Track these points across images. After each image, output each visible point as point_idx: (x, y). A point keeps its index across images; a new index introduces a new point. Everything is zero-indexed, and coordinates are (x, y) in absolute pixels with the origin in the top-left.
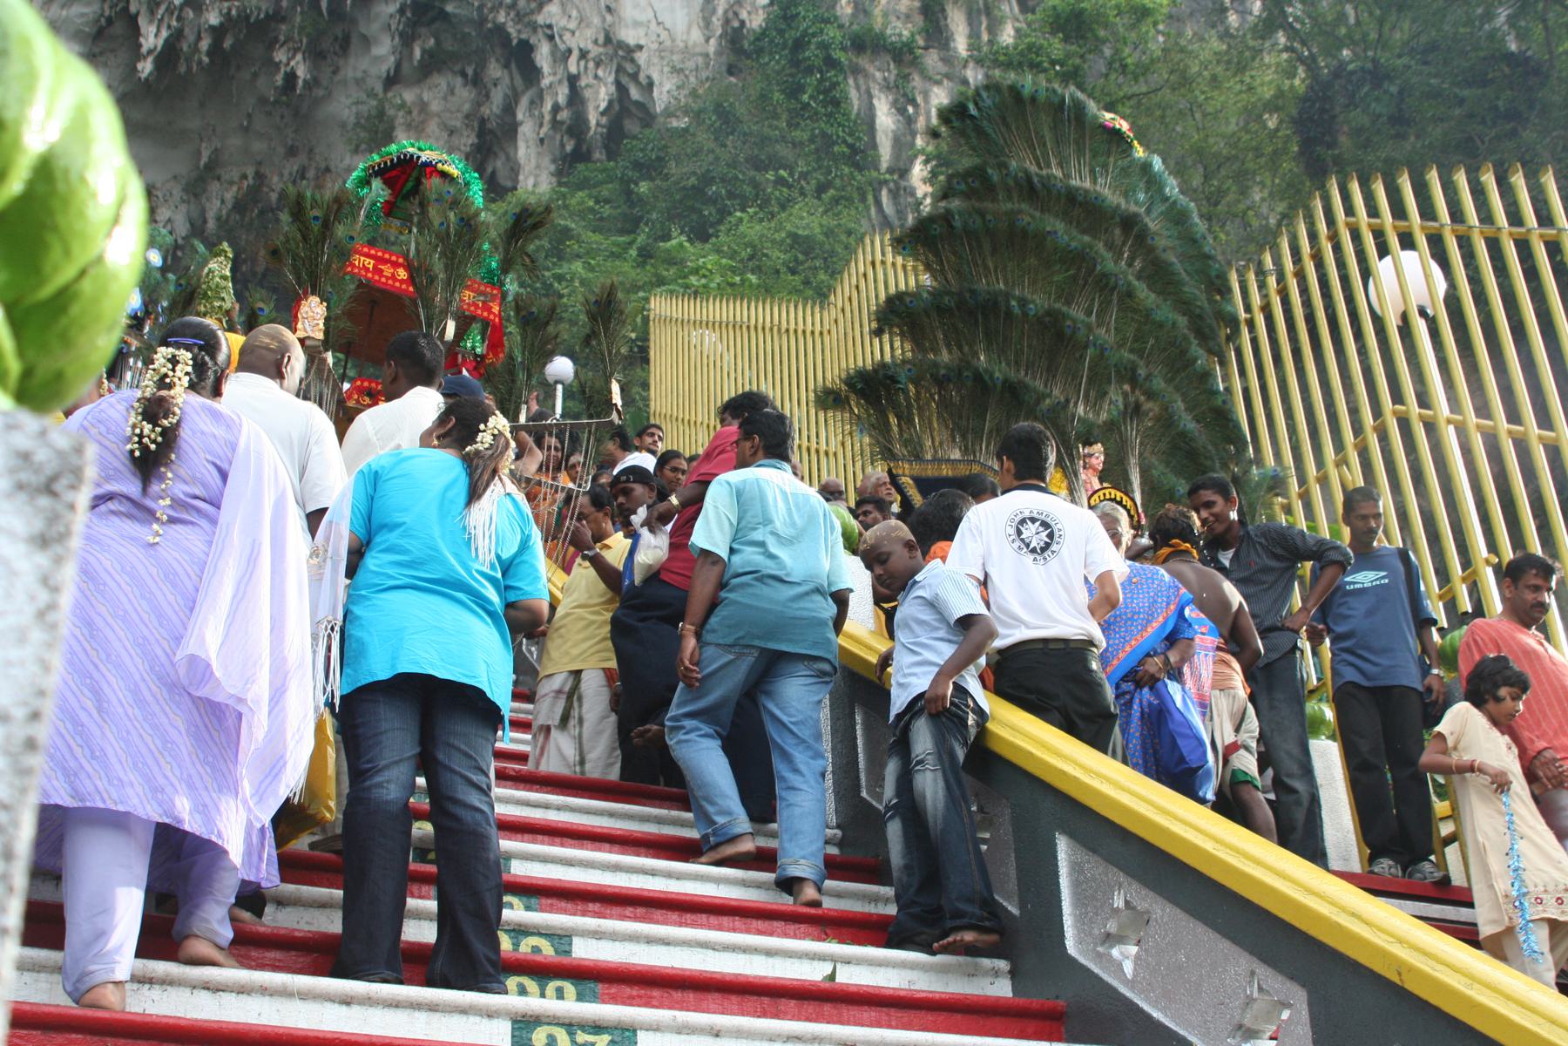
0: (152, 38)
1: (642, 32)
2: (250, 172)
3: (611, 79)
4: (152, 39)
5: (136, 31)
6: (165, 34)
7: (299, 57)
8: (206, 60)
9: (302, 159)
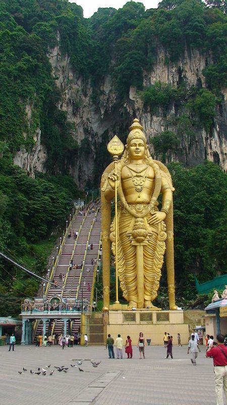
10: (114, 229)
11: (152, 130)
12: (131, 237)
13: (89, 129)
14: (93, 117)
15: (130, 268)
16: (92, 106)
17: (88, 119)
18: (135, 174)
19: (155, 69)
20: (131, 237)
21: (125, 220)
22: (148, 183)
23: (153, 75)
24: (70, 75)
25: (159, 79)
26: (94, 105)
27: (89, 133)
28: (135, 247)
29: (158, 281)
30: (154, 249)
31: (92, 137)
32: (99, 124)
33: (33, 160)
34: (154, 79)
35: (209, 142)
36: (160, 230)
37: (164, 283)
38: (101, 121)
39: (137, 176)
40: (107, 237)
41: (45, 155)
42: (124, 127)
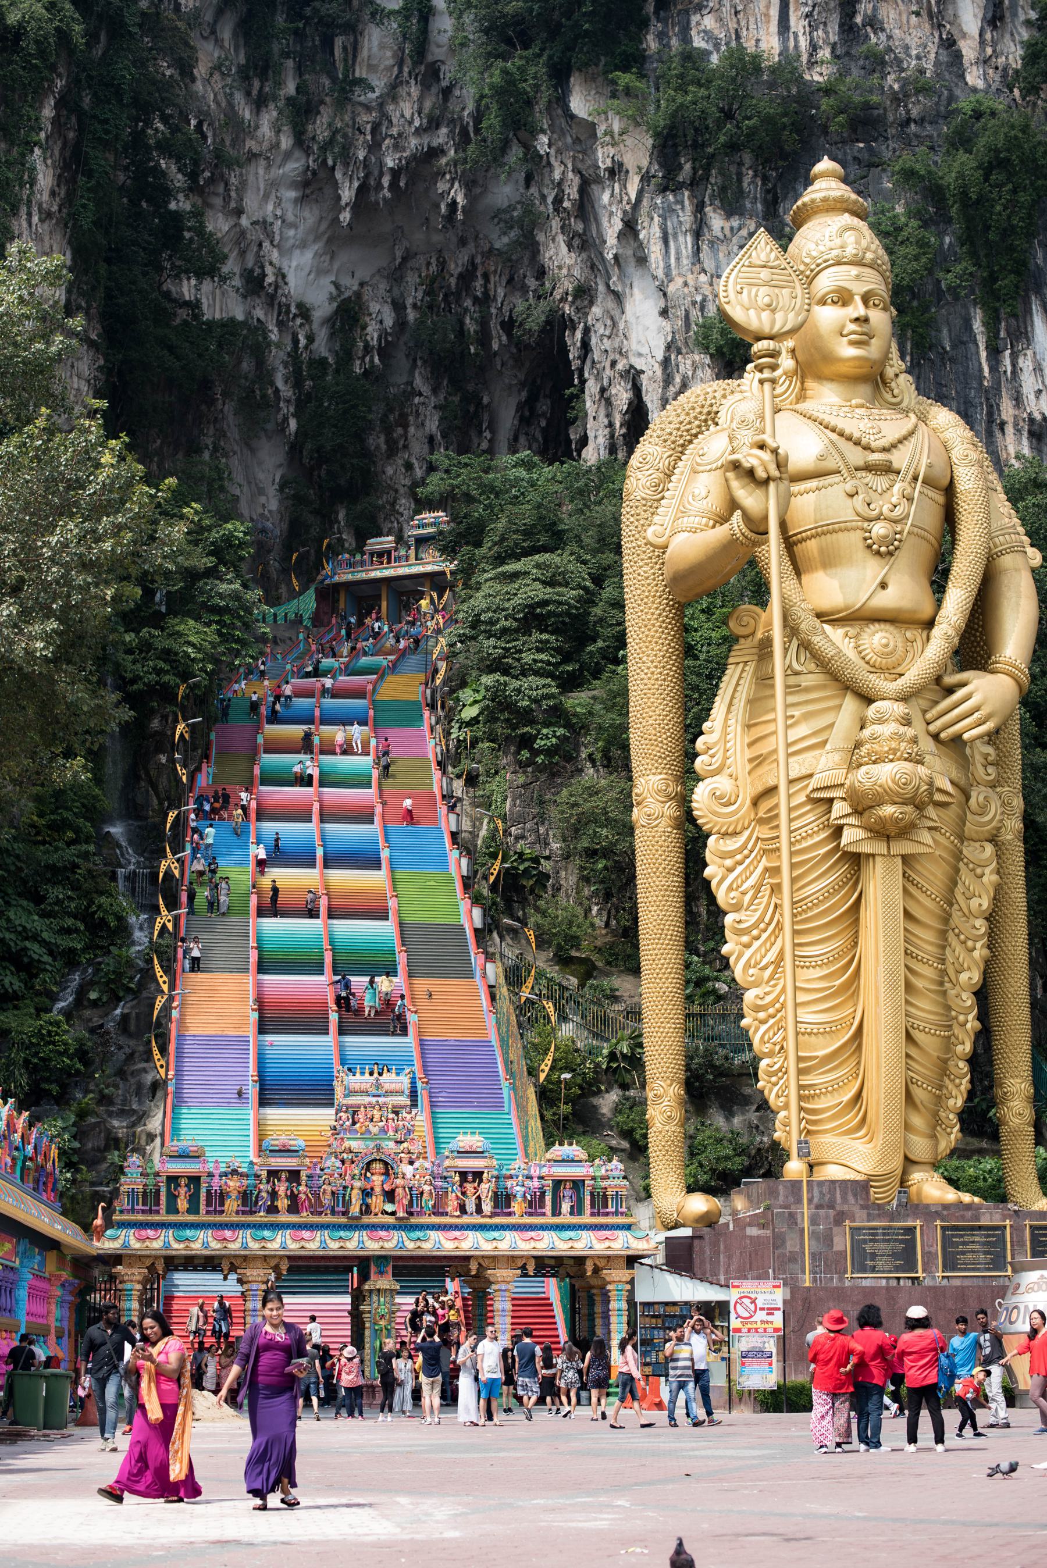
0: (347, 194)
1: (642, 360)
2: (433, 261)
3: (629, 386)
4: (347, 193)
5: (336, 185)
6: (356, 184)
7: (456, 185)
8: (388, 195)
9: (471, 246)
10: (717, 762)
11: (703, 278)
13: (270, 279)
14: (290, 217)
16: (288, 156)
17: (263, 224)
18: (857, 457)
20: (840, 808)
22: (924, 512)
25: (733, 25)
26: (297, 154)
27: (271, 300)
28: (855, 861)
31: (280, 324)
32: (316, 254)
34: (709, 22)
35: (1007, 362)
37: (983, 1064)
38: (334, 240)
39: (868, 468)
40: (670, 810)
42: (453, 281)
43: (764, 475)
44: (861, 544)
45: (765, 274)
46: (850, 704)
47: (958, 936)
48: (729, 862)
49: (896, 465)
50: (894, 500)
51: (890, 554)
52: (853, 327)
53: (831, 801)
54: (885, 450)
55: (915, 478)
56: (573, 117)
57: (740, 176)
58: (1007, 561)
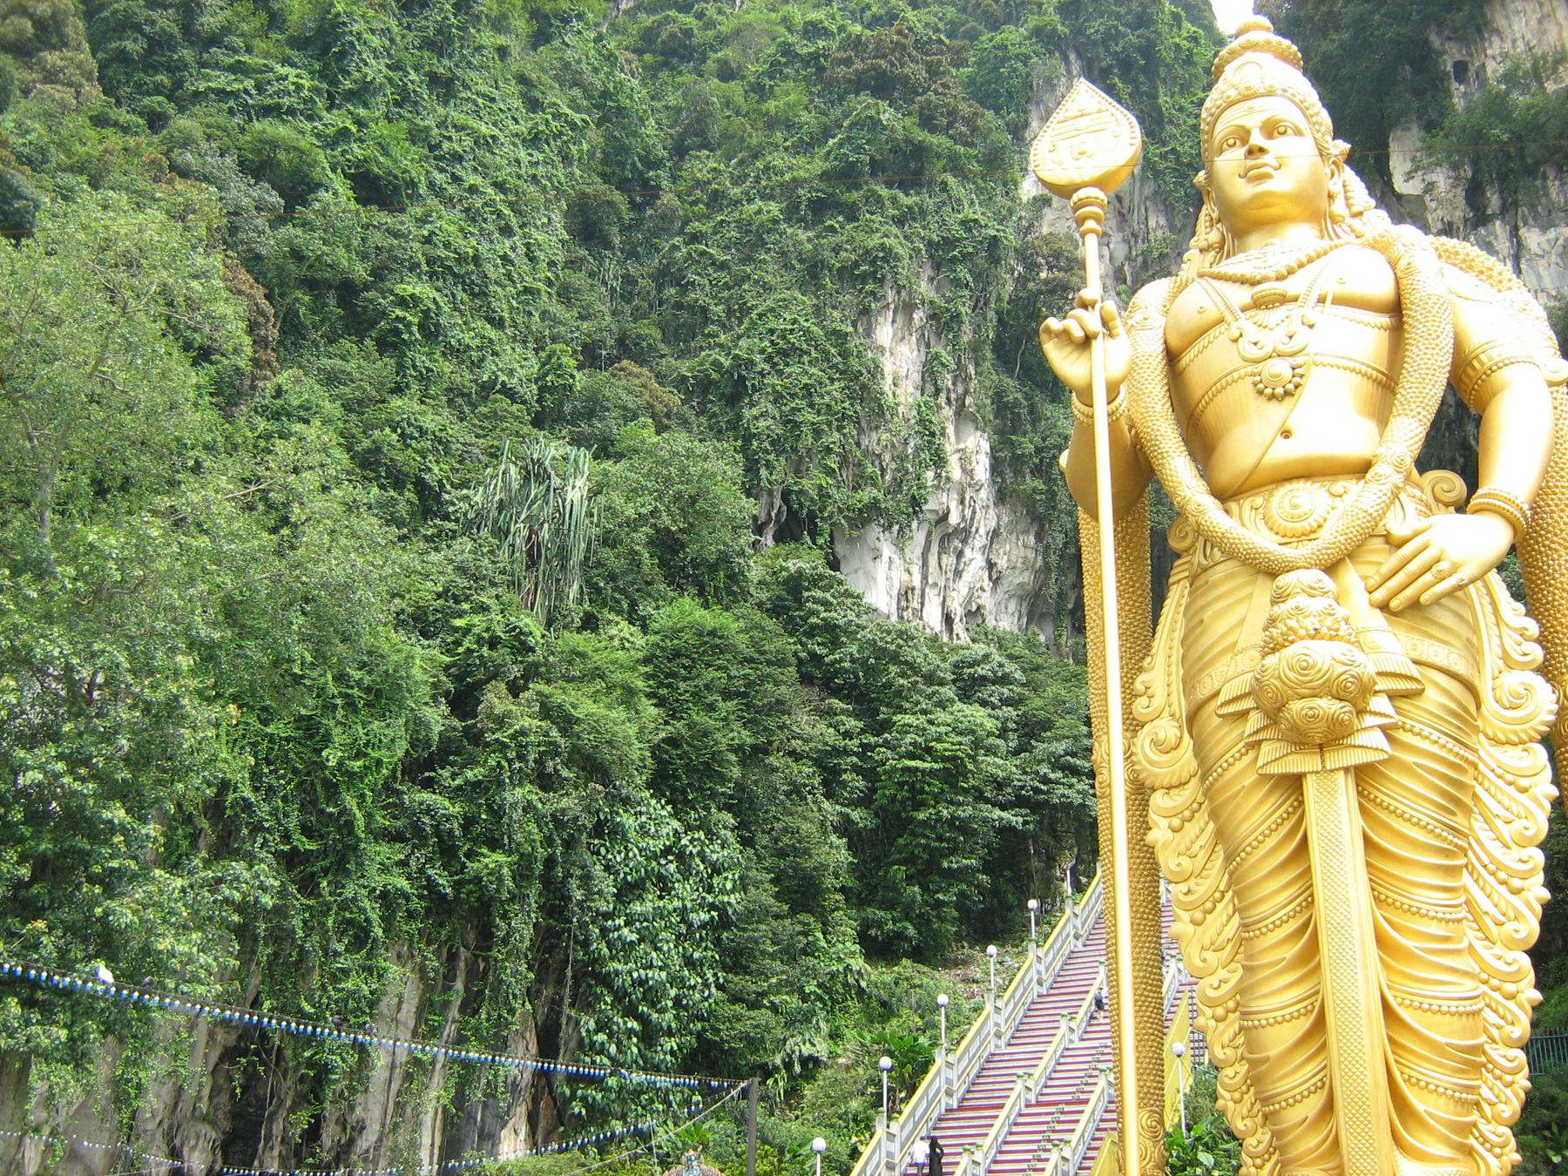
12: (1255, 721)
15: (1276, 948)
18: (1244, 295)
19: (1500, 21)
21: (1206, 615)
23: (1495, 47)
24: (1152, 223)
29: (1510, 1043)
30: (1456, 796)
33: (958, 574)
36: (1491, 660)
39: (1259, 304)
41: (1031, 555)
43: (1078, 334)
44: (1251, 391)
45: (1081, 123)
46: (1262, 591)
47: (1492, 874)
48: (1176, 822)
49: (1291, 292)
50: (1290, 331)
51: (1287, 394)
52: (1250, 163)
53: (1244, 714)
54: (1280, 278)
55: (1322, 300)
56: (1399, 197)
57: (1545, 187)
58: (1501, 376)
